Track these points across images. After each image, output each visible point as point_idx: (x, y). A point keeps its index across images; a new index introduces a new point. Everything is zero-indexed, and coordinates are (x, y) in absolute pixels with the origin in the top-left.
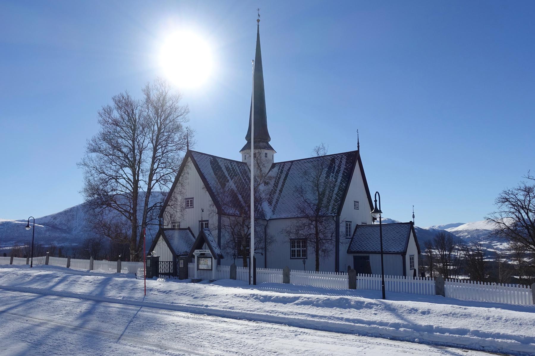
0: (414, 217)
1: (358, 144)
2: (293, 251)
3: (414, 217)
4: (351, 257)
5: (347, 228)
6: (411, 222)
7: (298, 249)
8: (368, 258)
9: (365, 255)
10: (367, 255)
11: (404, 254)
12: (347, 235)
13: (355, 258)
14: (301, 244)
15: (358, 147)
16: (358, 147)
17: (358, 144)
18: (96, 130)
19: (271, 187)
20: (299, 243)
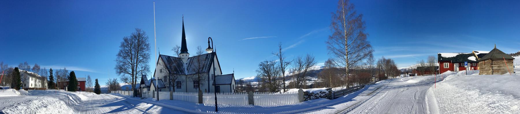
18: (118, 49)
19: (187, 65)
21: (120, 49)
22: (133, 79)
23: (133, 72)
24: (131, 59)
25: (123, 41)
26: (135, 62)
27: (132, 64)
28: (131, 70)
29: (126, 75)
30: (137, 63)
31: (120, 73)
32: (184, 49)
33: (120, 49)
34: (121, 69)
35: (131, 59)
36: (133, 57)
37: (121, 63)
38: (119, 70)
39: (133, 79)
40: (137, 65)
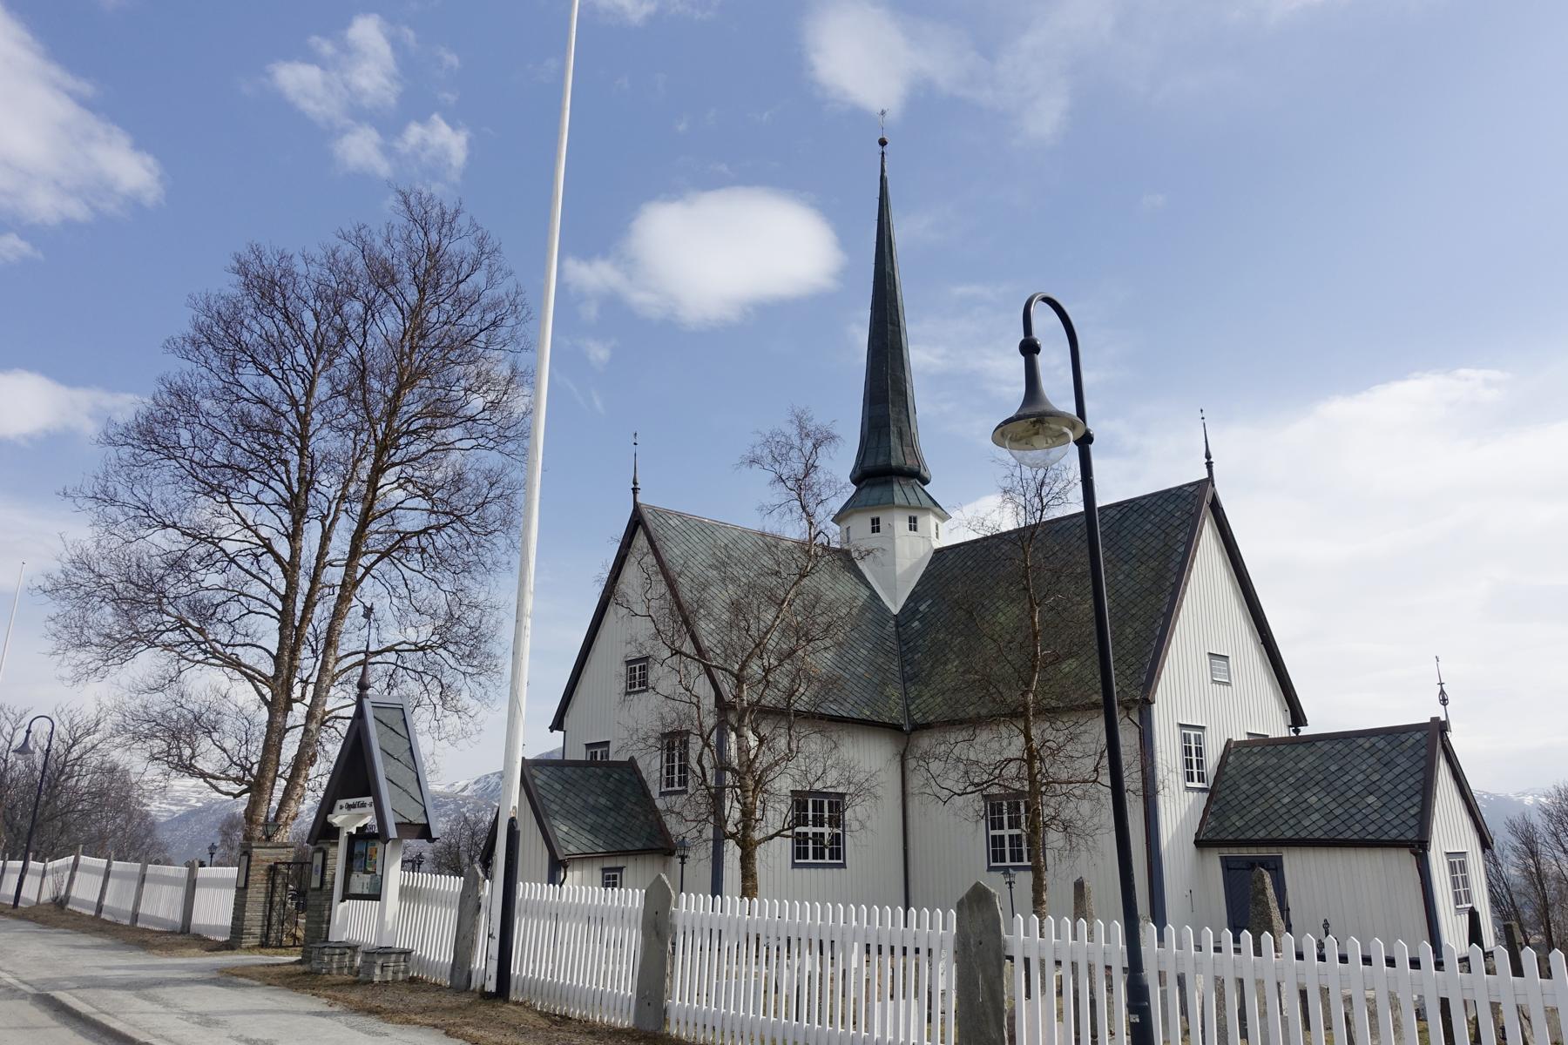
0: (1444, 701)
1: (1208, 456)
2: (997, 842)
3: (1444, 701)
4: (1213, 863)
5: (1187, 751)
6: (1435, 720)
7: (1016, 832)
8: (1276, 867)
9: (1264, 852)
10: (1274, 852)
11: (1419, 847)
12: (1190, 777)
13: (1226, 862)
14: (826, 815)
15: (1209, 465)
16: (1209, 465)
17: (1208, 456)
20: (818, 807)
21: (180, 368)
22: (275, 733)
23: (286, 658)
24: (296, 507)
25: (229, 286)
26: (340, 545)
27: (290, 569)
28: (268, 632)
29: (206, 683)
30: (355, 553)
31: (123, 645)
32: (887, 472)
33: (180, 368)
34: (141, 607)
35: (296, 507)
36: (328, 484)
37: (165, 541)
38: (107, 616)
39: (275, 733)
40: (349, 586)
